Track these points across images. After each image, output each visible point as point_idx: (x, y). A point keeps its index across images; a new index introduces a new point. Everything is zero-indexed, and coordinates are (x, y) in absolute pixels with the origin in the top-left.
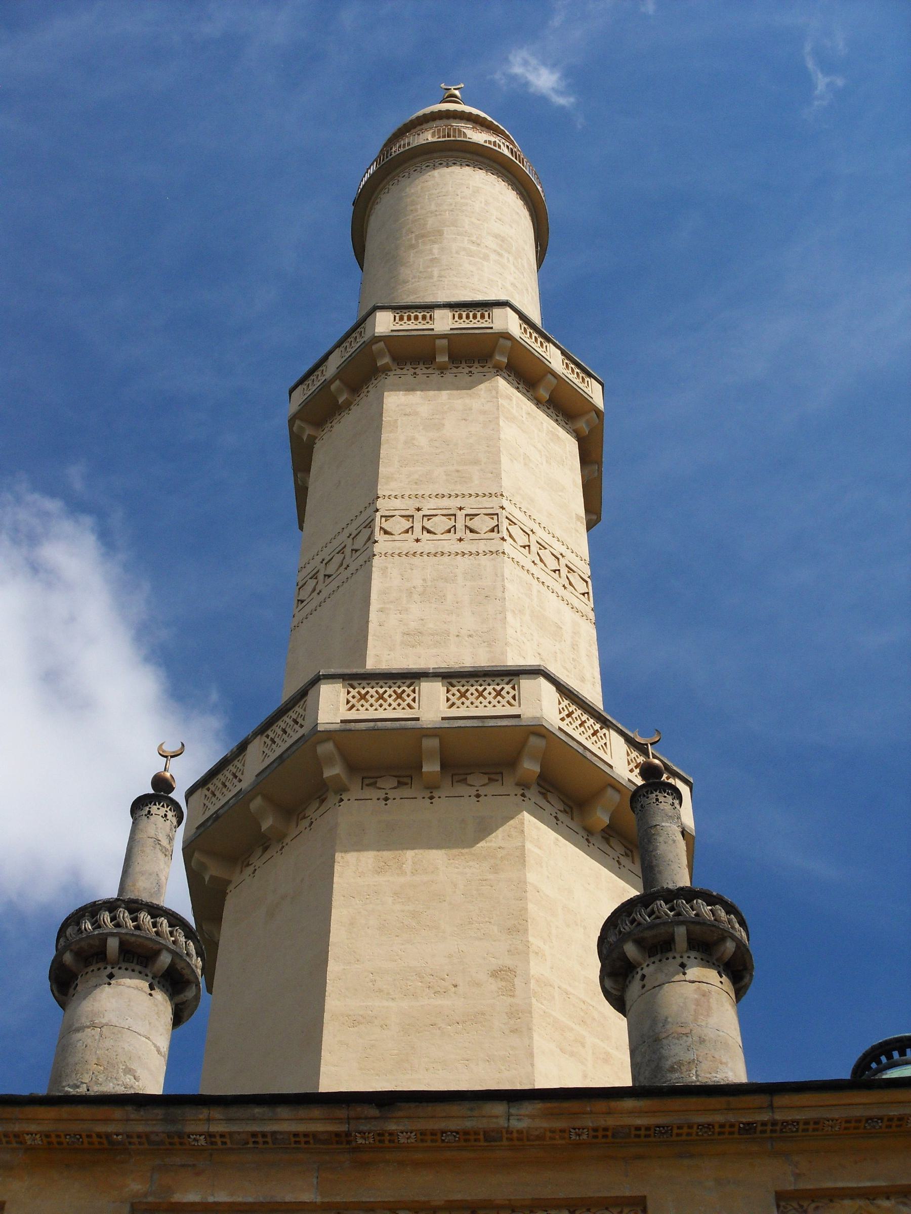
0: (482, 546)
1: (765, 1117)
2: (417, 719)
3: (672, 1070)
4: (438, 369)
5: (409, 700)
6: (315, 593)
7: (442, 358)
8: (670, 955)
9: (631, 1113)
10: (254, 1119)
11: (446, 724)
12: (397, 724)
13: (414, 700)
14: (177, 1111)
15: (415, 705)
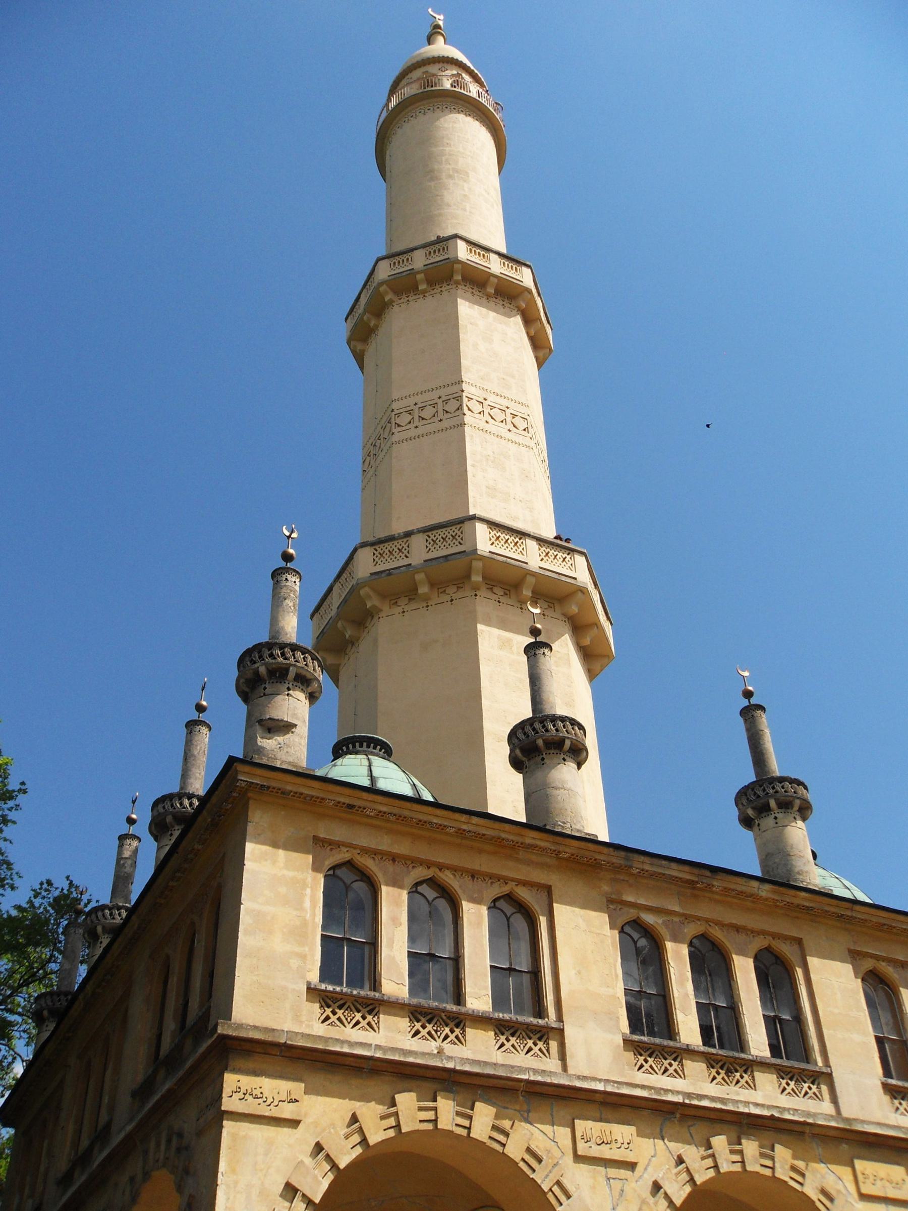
0: (520, 439)
1: (849, 913)
2: (527, 563)
3: (798, 873)
4: (486, 295)
5: (521, 549)
6: (412, 426)
7: (491, 290)
8: (789, 811)
9: (805, 899)
10: (661, 866)
11: (541, 572)
12: (517, 563)
13: (523, 549)
14: (630, 855)
15: (524, 553)
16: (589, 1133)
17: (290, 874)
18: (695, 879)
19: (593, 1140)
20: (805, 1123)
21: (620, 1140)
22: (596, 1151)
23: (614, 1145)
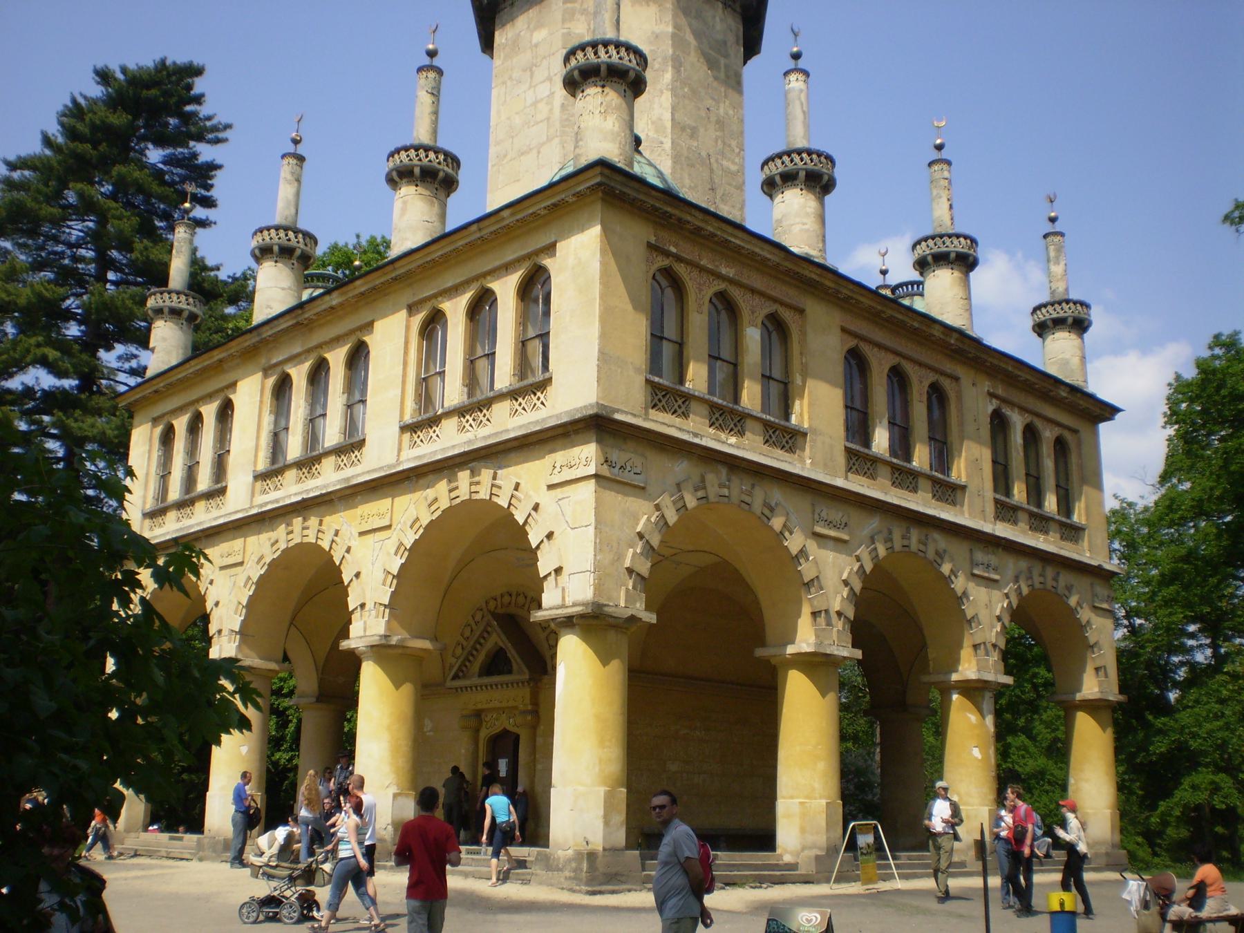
18: (294, 321)
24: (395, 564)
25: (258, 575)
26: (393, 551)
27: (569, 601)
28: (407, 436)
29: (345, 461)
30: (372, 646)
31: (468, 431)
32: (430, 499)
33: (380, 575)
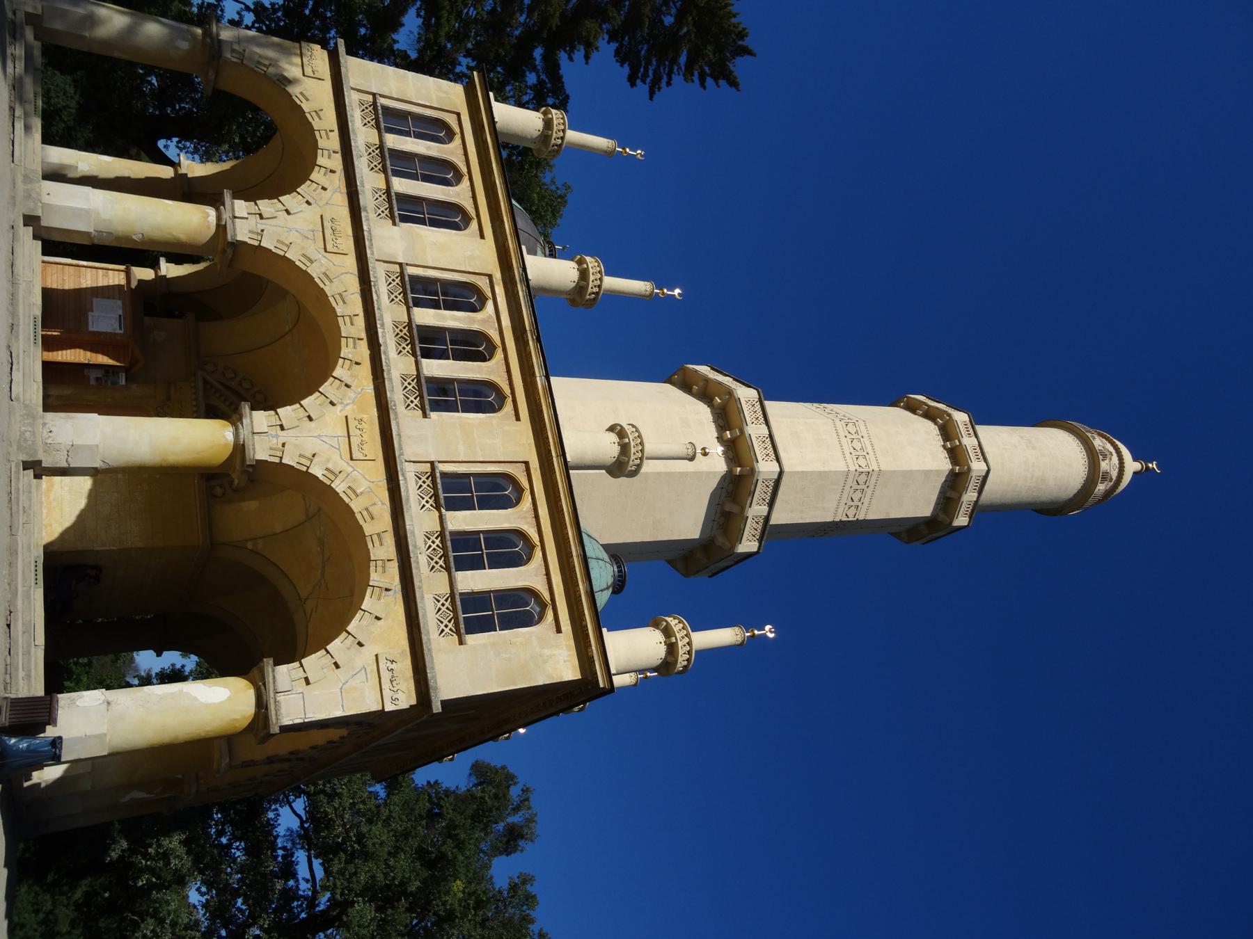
2: (747, 425)
16: (337, 223)
17: (434, 96)
19: (333, 225)
20: (382, 371)
21: (338, 242)
22: (327, 225)
23: (334, 237)
24: (317, 471)
25: (314, 275)
26: (330, 466)
27: (280, 697)
28: (427, 468)
29: (410, 387)
30: (243, 445)
31: (426, 544)
32: (373, 510)
33: (310, 446)
